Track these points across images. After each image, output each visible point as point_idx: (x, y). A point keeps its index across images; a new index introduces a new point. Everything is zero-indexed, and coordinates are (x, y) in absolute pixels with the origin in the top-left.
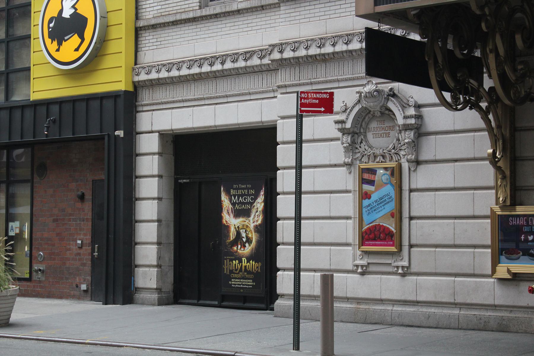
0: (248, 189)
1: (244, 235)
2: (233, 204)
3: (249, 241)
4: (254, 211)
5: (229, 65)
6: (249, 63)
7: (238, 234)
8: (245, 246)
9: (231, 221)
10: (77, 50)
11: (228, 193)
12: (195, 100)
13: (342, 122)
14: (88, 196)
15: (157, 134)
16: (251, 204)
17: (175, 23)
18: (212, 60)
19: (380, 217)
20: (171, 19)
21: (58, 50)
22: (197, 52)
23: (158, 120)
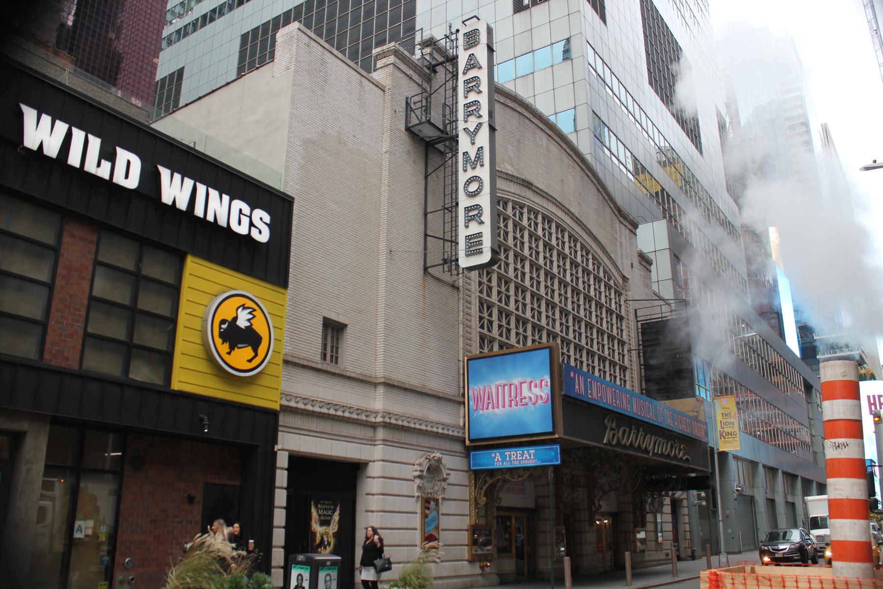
0: (330, 505)
1: (326, 539)
2: (320, 516)
3: (329, 544)
4: (332, 522)
5: (347, 414)
6: (359, 417)
7: (322, 539)
8: (325, 548)
9: (317, 528)
10: (250, 361)
11: (316, 507)
12: (318, 432)
13: (422, 471)
14: (199, 498)
15: (287, 453)
16: (331, 516)
17: (304, 367)
18: (336, 406)
19: (430, 529)
20: (305, 363)
21: (229, 353)
22: (320, 396)
23: (291, 442)
